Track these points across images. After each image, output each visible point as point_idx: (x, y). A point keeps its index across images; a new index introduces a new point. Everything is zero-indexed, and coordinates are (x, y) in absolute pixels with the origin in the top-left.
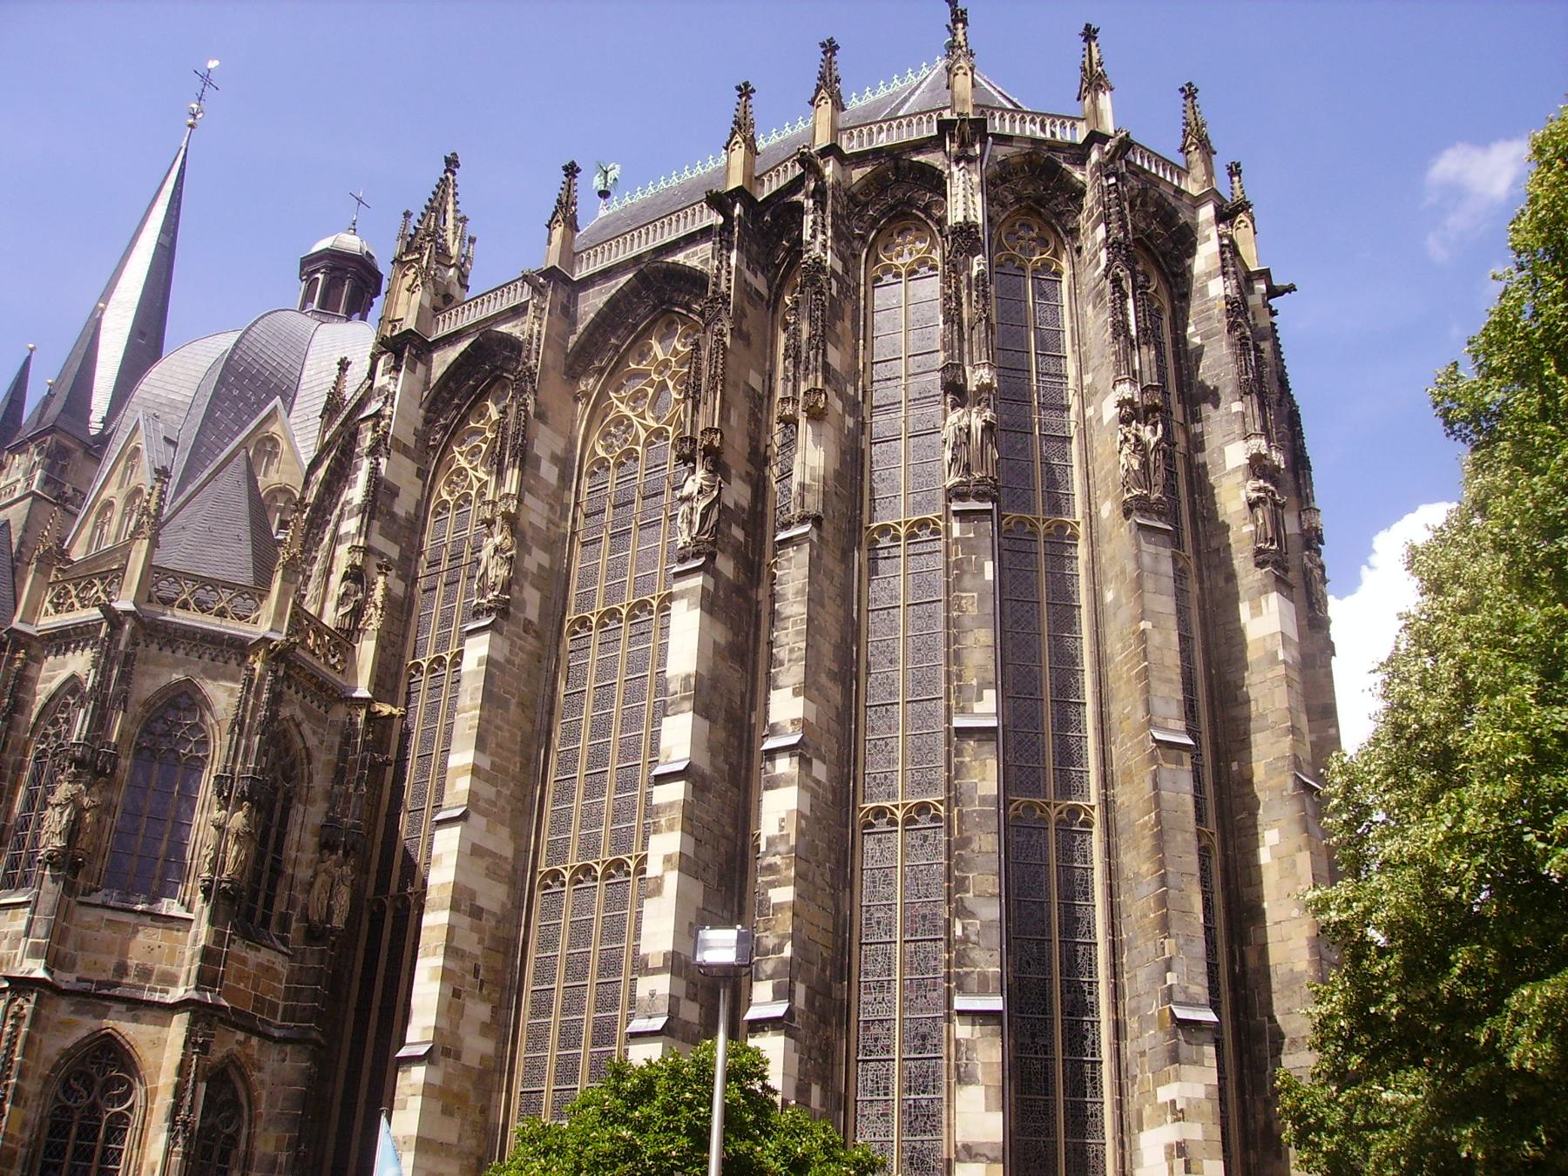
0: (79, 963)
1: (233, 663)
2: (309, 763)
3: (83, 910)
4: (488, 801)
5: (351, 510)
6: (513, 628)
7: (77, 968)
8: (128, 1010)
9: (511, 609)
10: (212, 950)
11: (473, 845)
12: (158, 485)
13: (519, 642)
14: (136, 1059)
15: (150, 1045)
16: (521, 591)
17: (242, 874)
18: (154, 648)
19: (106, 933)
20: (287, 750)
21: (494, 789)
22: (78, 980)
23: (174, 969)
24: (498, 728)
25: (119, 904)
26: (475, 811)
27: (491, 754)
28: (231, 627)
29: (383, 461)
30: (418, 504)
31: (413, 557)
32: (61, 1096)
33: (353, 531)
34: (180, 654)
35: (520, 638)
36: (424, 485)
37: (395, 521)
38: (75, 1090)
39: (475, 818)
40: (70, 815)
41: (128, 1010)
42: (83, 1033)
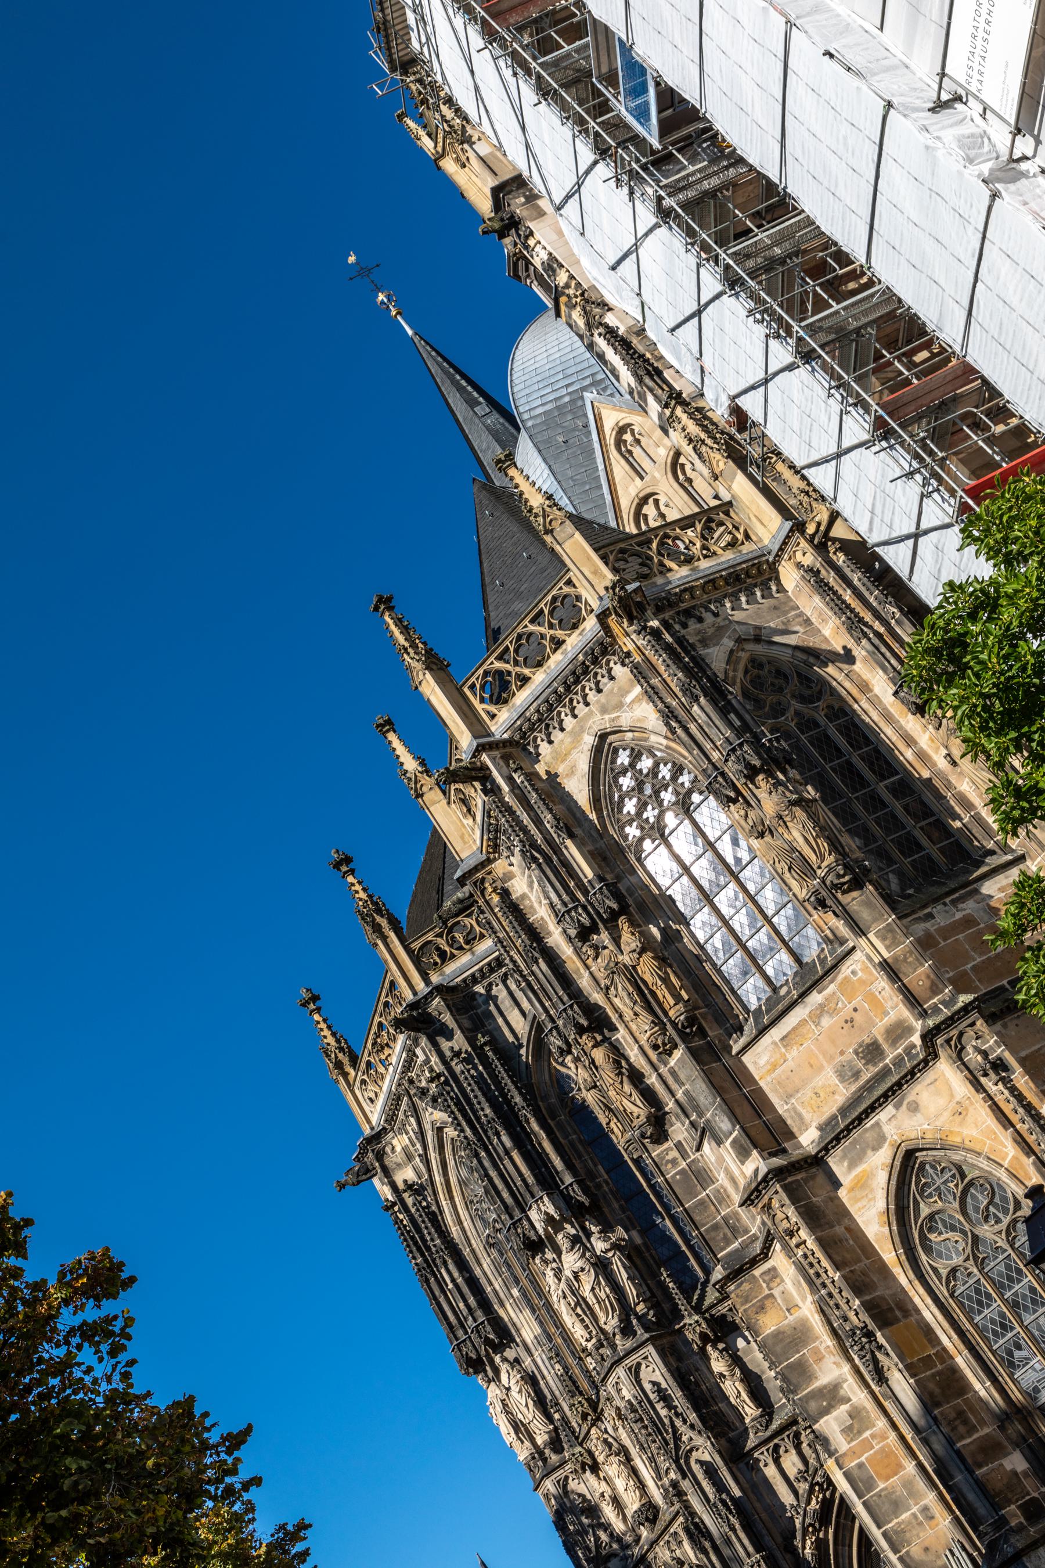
0: (804, 1112)
1: (618, 670)
3: (746, 1059)
7: (807, 1116)
8: (897, 1107)
10: (896, 959)
15: (958, 1118)
17: (835, 846)
18: (544, 748)
19: (793, 1054)
20: (779, 673)
22: (820, 1128)
23: (892, 1017)
25: (775, 1013)
28: (574, 642)
29: (610, 319)
34: (569, 722)
40: (624, 988)
41: (897, 1107)
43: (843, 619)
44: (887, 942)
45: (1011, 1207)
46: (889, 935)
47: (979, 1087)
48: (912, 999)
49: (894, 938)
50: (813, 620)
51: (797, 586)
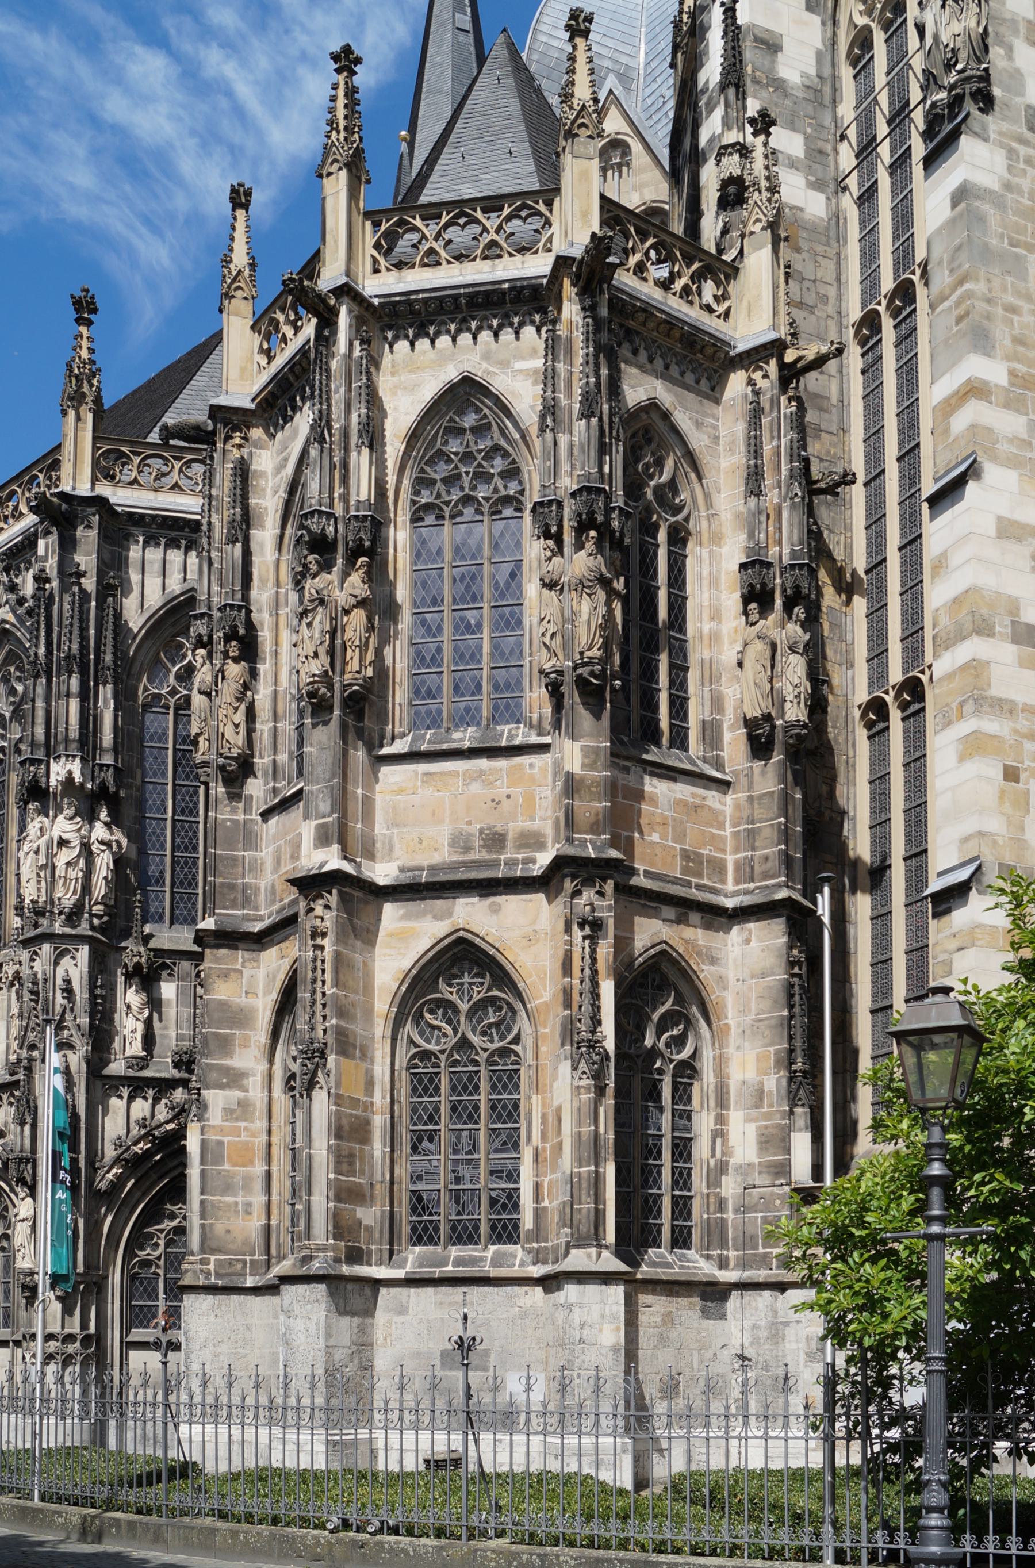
2: (700, 478)
4: (1013, 440)
5: (707, 104)
6: (1005, 126)
9: (997, 91)
10: (582, 779)
11: (1000, 519)
12: (341, 79)
13: (1023, 150)
14: (508, 967)
15: (525, 942)
16: (1010, 57)
21: (1022, 420)
24: (1012, 309)
26: (995, 459)
27: (1008, 358)
30: (819, 55)
31: (829, 148)
32: (418, 1040)
33: (719, 131)
35: (1022, 141)
36: (823, 23)
37: (786, 95)
38: (434, 1028)
39: (990, 470)
42: (425, 943)
43: (752, 462)
44: (586, 761)
45: (510, 1038)
46: (593, 756)
47: (568, 929)
48: (570, 821)
49: (595, 762)
50: (721, 442)
51: (734, 399)
